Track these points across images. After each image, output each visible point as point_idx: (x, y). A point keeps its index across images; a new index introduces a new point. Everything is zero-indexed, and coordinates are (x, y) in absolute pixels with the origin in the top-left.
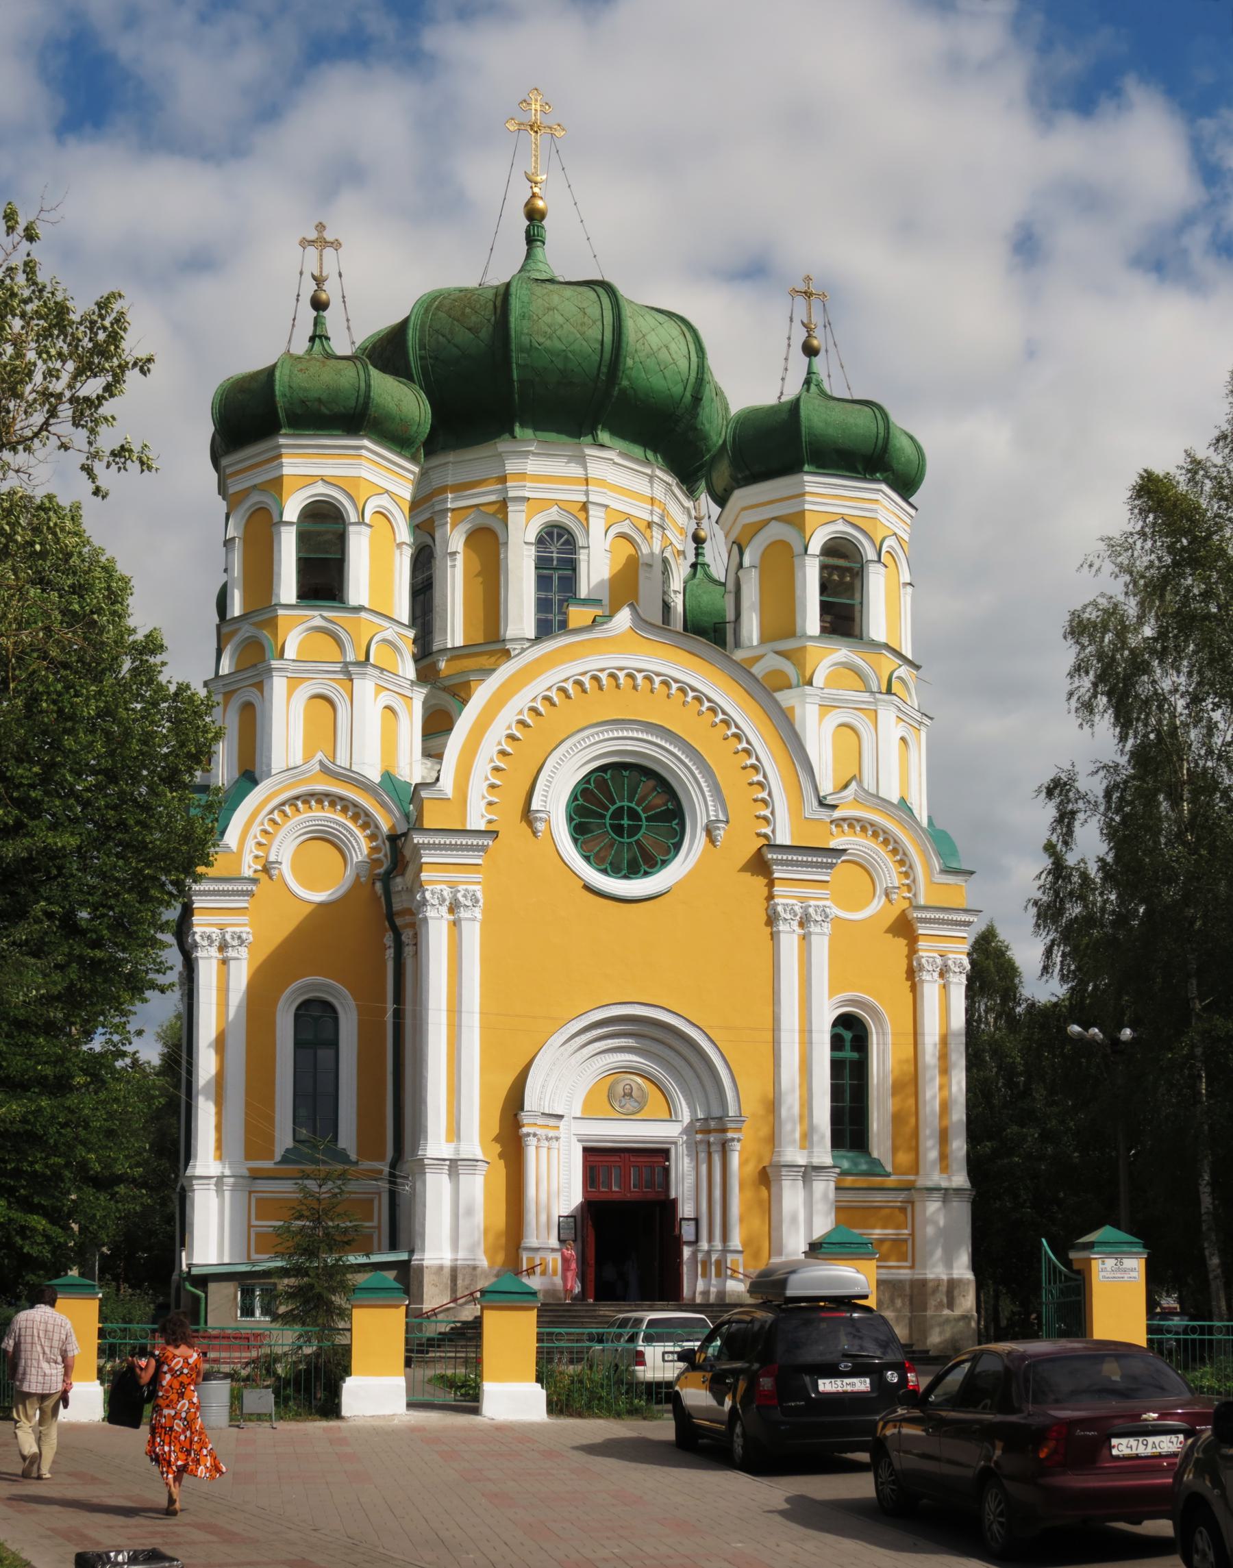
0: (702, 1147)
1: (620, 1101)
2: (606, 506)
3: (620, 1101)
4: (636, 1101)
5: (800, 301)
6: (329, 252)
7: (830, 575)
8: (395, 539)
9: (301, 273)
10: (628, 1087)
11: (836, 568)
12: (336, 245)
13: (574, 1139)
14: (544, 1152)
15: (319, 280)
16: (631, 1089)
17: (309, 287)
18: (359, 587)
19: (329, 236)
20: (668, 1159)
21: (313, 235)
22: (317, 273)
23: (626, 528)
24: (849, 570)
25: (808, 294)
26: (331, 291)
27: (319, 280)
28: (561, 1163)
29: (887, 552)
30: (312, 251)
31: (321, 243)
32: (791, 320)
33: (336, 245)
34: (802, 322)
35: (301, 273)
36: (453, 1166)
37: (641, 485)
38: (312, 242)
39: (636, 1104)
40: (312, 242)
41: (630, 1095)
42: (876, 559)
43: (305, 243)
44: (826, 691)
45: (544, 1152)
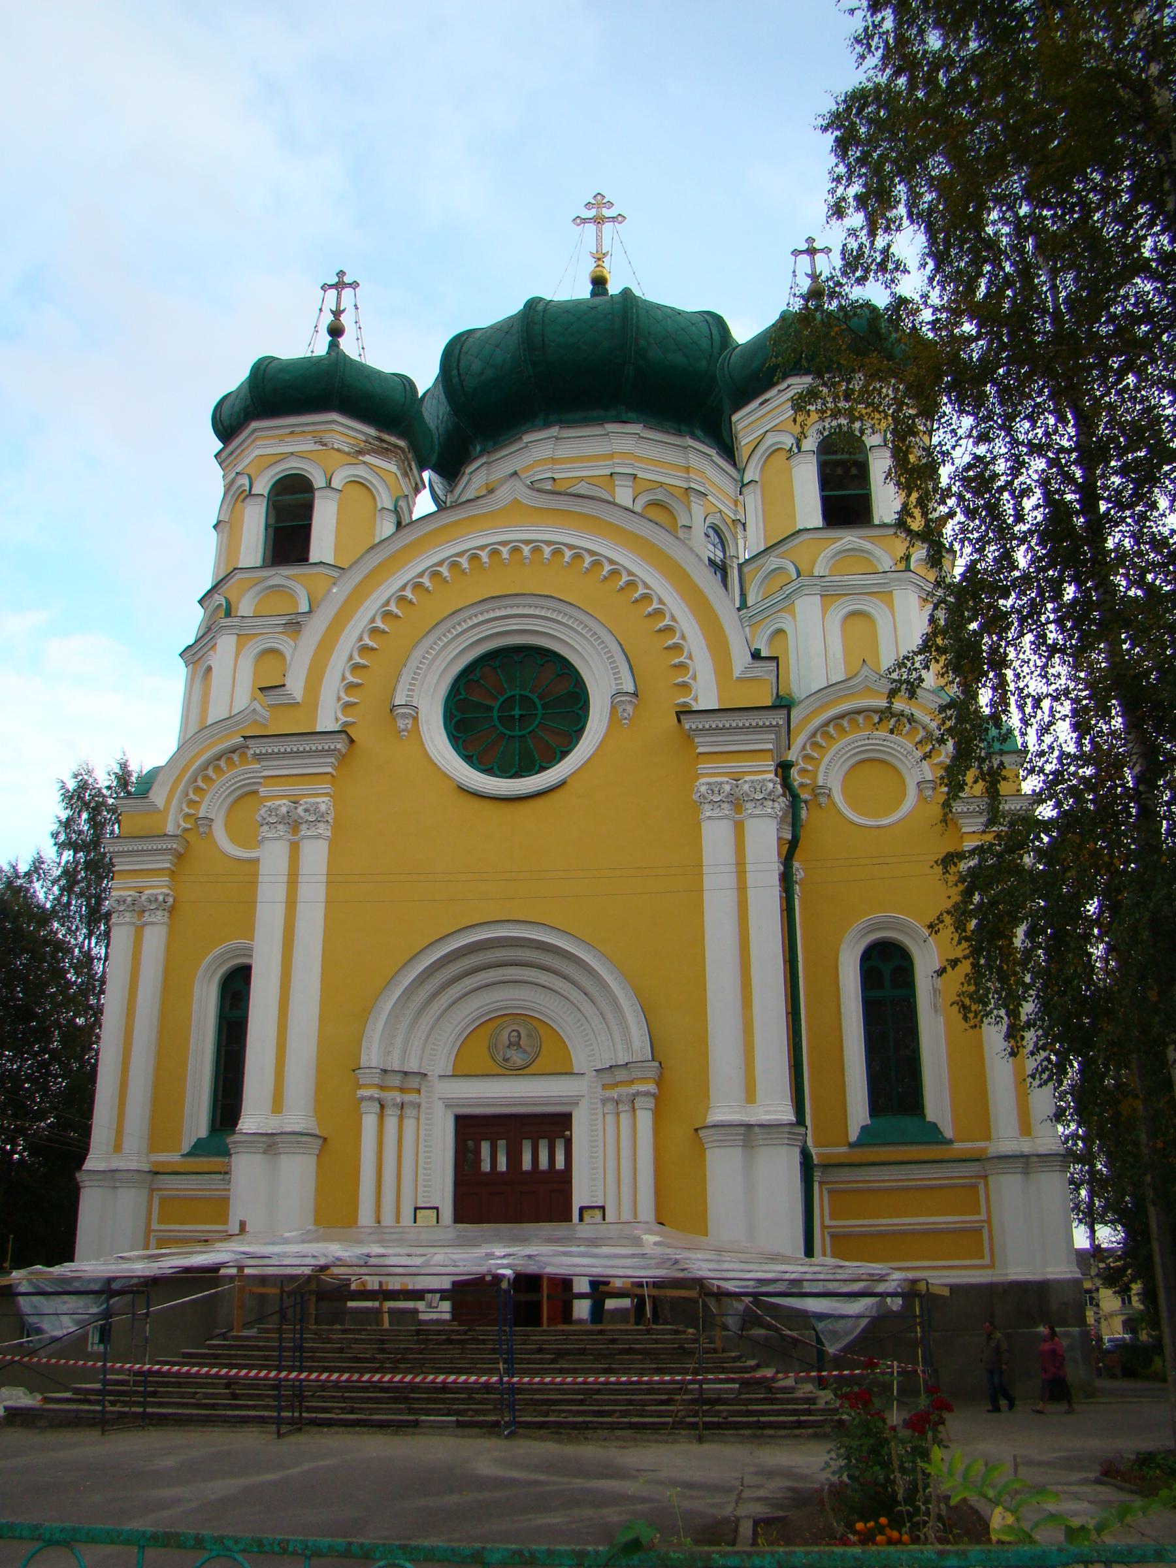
0: (610, 1107)
2: (635, 476)
5: (805, 258)
6: (347, 293)
8: (376, 506)
9: (321, 310)
10: (514, 1034)
12: (354, 285)
13: (439, 1107)
15: (337, 313)
16: (519, 1036)
18: (322, 545)
19: (347, 280)
22: (334, 309)
23: (659, 496)
25: (811, 252)
27: (337, 313)
31: (340, 286)
33: (354, 285)
34: (808, 275)
35: (321, 310)
36: (271, 1143)
37: (672, 457)
38: (331, 286)
40: (331, 286)
41: (518, 1044)
45: (391, 1123)
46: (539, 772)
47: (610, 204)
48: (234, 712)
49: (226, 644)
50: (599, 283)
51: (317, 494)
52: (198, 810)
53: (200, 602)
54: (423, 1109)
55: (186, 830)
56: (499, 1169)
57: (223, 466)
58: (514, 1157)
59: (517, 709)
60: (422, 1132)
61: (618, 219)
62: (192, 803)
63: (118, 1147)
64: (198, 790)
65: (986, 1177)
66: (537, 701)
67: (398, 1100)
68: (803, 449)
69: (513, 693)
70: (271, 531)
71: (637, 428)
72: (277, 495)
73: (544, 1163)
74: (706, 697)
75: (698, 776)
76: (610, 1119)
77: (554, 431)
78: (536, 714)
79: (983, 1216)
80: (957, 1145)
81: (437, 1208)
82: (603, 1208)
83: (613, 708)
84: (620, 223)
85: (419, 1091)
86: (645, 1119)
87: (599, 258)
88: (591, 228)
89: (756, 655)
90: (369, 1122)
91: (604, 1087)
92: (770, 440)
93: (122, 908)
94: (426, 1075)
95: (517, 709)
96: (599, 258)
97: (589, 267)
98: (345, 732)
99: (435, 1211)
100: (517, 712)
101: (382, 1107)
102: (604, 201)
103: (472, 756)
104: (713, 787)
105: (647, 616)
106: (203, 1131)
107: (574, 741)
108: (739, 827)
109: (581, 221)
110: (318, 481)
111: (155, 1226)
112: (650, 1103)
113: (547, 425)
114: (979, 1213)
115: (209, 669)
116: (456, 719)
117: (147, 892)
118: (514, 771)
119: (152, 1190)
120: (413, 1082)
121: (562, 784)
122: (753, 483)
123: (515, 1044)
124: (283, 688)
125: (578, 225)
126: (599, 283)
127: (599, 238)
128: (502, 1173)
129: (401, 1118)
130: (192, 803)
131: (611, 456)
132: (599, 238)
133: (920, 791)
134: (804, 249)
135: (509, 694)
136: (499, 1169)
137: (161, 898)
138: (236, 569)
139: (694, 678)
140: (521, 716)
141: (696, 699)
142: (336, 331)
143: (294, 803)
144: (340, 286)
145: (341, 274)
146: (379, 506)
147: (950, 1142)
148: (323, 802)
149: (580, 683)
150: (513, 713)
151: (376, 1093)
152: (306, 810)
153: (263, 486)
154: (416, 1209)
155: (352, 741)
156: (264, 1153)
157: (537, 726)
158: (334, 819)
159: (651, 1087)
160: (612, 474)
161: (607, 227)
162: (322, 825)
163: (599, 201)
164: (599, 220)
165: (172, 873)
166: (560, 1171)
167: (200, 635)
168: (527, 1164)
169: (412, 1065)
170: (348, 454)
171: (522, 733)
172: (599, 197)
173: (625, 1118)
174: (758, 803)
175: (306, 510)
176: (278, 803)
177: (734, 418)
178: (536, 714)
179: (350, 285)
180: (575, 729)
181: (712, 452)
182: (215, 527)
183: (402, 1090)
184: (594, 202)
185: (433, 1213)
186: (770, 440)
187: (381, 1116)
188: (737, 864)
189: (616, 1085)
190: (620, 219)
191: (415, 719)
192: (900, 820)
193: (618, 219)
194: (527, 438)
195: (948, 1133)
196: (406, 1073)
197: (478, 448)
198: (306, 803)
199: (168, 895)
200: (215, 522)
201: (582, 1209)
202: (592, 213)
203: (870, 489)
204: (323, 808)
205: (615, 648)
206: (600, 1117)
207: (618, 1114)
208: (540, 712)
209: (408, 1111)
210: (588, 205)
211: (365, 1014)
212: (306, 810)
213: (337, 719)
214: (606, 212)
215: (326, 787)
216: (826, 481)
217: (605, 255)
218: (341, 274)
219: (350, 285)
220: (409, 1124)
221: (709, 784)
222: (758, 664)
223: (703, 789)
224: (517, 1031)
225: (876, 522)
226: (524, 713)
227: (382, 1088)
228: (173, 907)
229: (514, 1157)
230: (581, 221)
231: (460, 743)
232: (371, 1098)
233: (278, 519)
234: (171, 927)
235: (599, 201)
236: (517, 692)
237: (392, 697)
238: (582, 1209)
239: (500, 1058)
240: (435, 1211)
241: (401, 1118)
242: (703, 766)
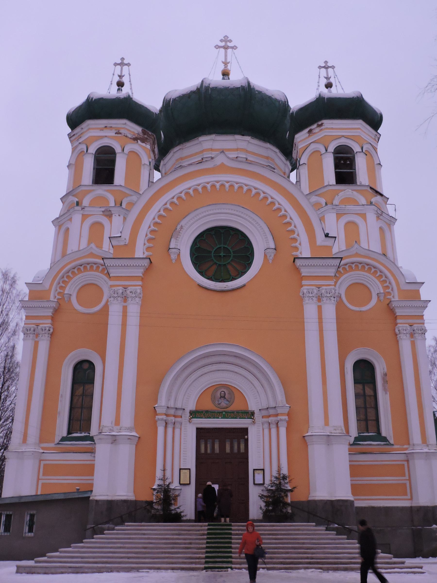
0: (266, 426)
1: (218, 401)
3: (218, 401)
4: (227, 401)
5: (323, 70)
6: (125, 68)
7: (340, 161)
9: (113, 74)
10: (223, 393)
11: (342, 158)
14: (170, 430)
15: (121, 76)
17: (117, 79)
19: (126, 62)
20: (247, 434)
21: (119, 61)
22: (119, 74)
24: (348, 158)
25: (326, 67)
26: (125, 80)
28: (182, 435)
29: (366, 151)
30: (119, 67)
31: (122, 64)
32: (319, 77)
33: (128, 65)
35: (113, 74)
39: (227, 402)
41: (224, 397)
42: (361, 151)
43: (116, 64)
44: (340, 206)
45: (170, 430)
46: (231, 281)
47: (230, 41)
48: (81, 248)
49: (77, 218)
50: (225, 74)
51: (118, 156)
52: (64, 291)
53: (61, 199)
54: (183, 425)
55: (58, 299)
56: (216, 452)
57: (72, 139)
58: (222, 447)
59: (222, 253)
60: (182, 435)
61: (235, 48)
62: (61, 287)
63: (25, 440)
64: (64, 282)
65: (408, 461)
66: (231, 250)
67: (174, 421)
68: (328, 151)
69: (220, 246)
70: (95, 169)
71: (248, 138)
72: (98, 154)
73: (228, 450)
74: (306, 252)
75: (302, 286)
76: (266, 431)
77: (213, 136)
78: (231, 256)
79: (407, 477)
80: (395, 447)
81: (190, 469)
82: (263, 470)
83: (265, 255)
84: (235, 49)
85: (181, 417)
86: (283, 431)
87: (226, 63)
88: (222, 50)
89: (327, 235)
90: (161, 430)
91: (263, 417)
92: (313, 147)
93: (29, 332)
94: (184, 409)
95: (222, 253)
96: (226, 63)
97: (221, 67)
98: (149, 258)
99: (189, 470)
100: (222, 254)
101: (166, 423)
102: (228, 39)
103: (203, 272)
104: (309, 291)
105: (279, 217)
106: (65, 434)
107: (247, 268)
108: (320, 308)
109: (217, 47)
110: (118, 149)
111: (41, 476)
112: (286, 424)
113: (210, 133)
114: (405, 476)
115: (68, 229)
116: (195, 256)
117: (41, 326)
118: (221, 279)
119: (40, 460)
120: (179, 413)
121: (244, 286)
122: (304, 164)
123: (223, 397)
124: (120, 238)
125: (217, 49)
126: (225, 74)
127: (226, 56)
128: (217, 454)
129: (174, 428)
130: (61, 287)
131: (237, 150)
132: (226, 56)
133: (378, 297)
134: (323, 66)
135: (218, 246)
136: (216, 452)
137: (48, 329)
138: (81, 185)
139: (300, 244)
140: (224, 256)
141: (301, 253)
142: (120, 84)
143: (125, 288)
144: (122, 64)
145: (123, 59)
146: (143, 163)
147: (393, 445)
148: (139, 290)
149: (250, 243)
150: (220, 254)
151: (164, 417)
152: (131, 292)
153: (93, 149)
154: (180, 469)
155: (151, 262)
156: (112, 443)
157: (231, 261)
158: (143, 296)
159: (286, 418)
160: (237, 157)
161: (229, 51)
162: (137, 299)
163: (226, 39)
164: (226, 48)
165: (53, 318)
166: (243, 453)
167: (62, 214)
168: (228, 450)
169: (179, 406)
170: (131, 138)
171: (224, 263)
172: (226, 37)
173: (274, 431)
174: (328, 298)
175: (113, 162)
176: (118, 288)
177: (296, 136)
178: (231, 256)
179: (126, 65)
180: (247, 263)
181: (277, 150)
182: (68, 166)
183: (175, 416)
184: (224, 39)
185: (187, 471)
186: (313, 147)
187: (166, 427)
188: (322, 322)
189: (269, 416)
190: (235, 48)
191: (179, 255)
192: (370, 309)
193: (235, 48)
194: (202, 138)
195: (392, 442)
196: (176, 409)
197: (177, 142)
198: (131, 289)
199: (50, 327)
200: (68, 164)
201: (254, 470)
202: (223, 44)
203: (355, 169)
204: (139, 291)
205: (267, 230)
206: (261, 430)
207: (270, 430)
208: (232, 254)
209: (177, 425)
210: (221, 41)
211: (159, 383)
212: (131, 292)
213: (144, 253)
214: (229, 44)
215: (140, 283)
216: (337, 166)
217: (229, 63)
218: (123, 59)
219: (126, 65)
220: (177, 431)
221: (308, 289)
222: (328, 238)
223: (305, 291)
224: (224, 392)
225: (358, 184)
226: (225, 255)
227: (167, 415)
228: (52, 333)
229: (222, 447)
230: (217, 47)
231: (197, 266)
232: (162, 419)
233: (97, 165)
234: (51, 342)
235: (226, 39)
236: (222, 246)
237: (169, 245)
238: (254, 470)
239: (217, 402)
240: (189, 470)
241: (174, 428)
242: (304, 282)
